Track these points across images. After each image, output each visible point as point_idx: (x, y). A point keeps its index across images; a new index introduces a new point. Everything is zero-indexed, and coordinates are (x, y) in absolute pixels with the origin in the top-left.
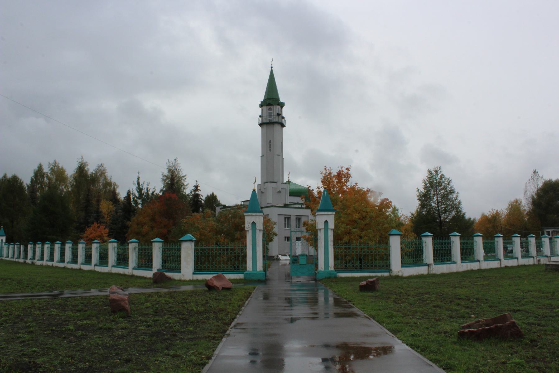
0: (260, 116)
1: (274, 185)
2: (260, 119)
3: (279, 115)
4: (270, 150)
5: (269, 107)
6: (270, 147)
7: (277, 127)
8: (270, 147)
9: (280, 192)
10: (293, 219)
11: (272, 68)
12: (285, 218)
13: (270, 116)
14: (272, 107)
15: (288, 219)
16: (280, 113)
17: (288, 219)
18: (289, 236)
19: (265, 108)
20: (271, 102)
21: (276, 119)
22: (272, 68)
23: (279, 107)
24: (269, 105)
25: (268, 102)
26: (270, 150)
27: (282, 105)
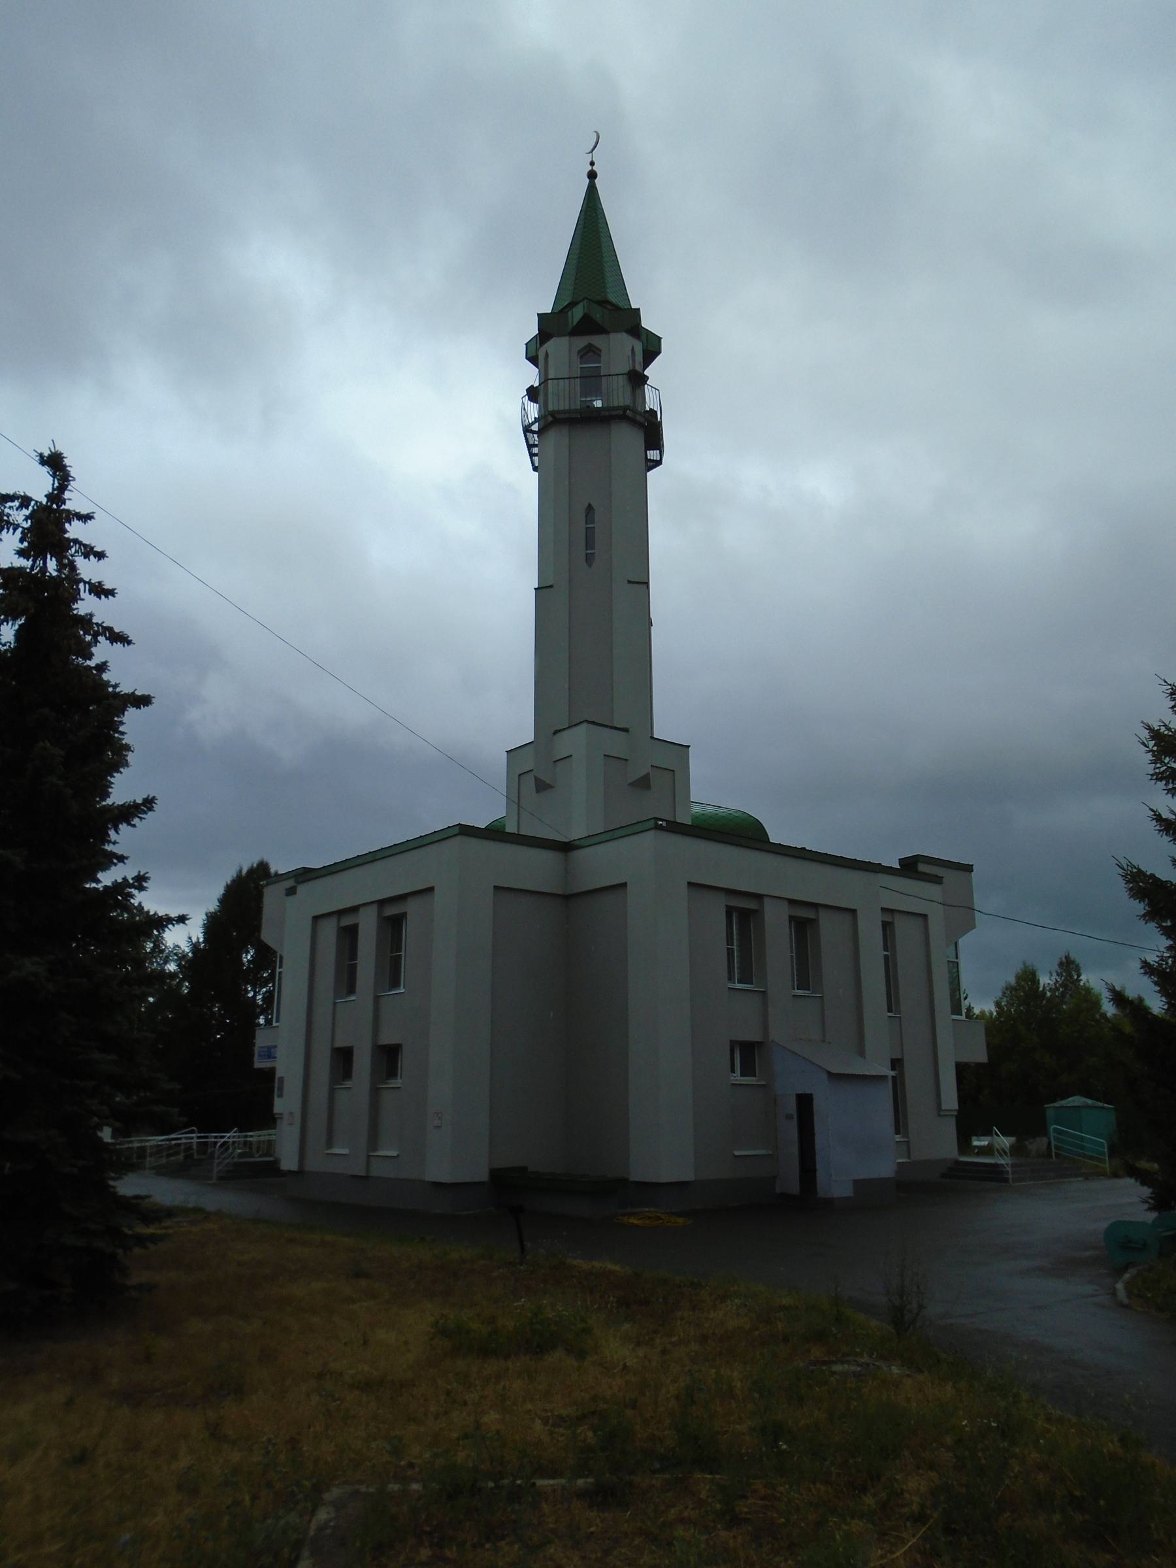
0: (532, 394)
1: (615, 743)
2: (533, 410)
3: (638, 380)
4: (589, 559)
5: (581, 342)
6: (590, 541)
7: (627, 438)
8: (590, 541)
9: (643, 783)
10: (776, 925)
11: (592, 175)
12: (729, 911)
13: (591, 380)
14: (597, 340)
15: (744, 914)
16: (639, 368)
17: (744, 914)
18: (753, 1036)
19: (558, 347)
20: (598, 315)
21: (621, 397)
22: (592, 175)
23: (639, 347)
24: (588, 326)
25: (578, 313)
26: (589, 559)
27: (651, 348)
